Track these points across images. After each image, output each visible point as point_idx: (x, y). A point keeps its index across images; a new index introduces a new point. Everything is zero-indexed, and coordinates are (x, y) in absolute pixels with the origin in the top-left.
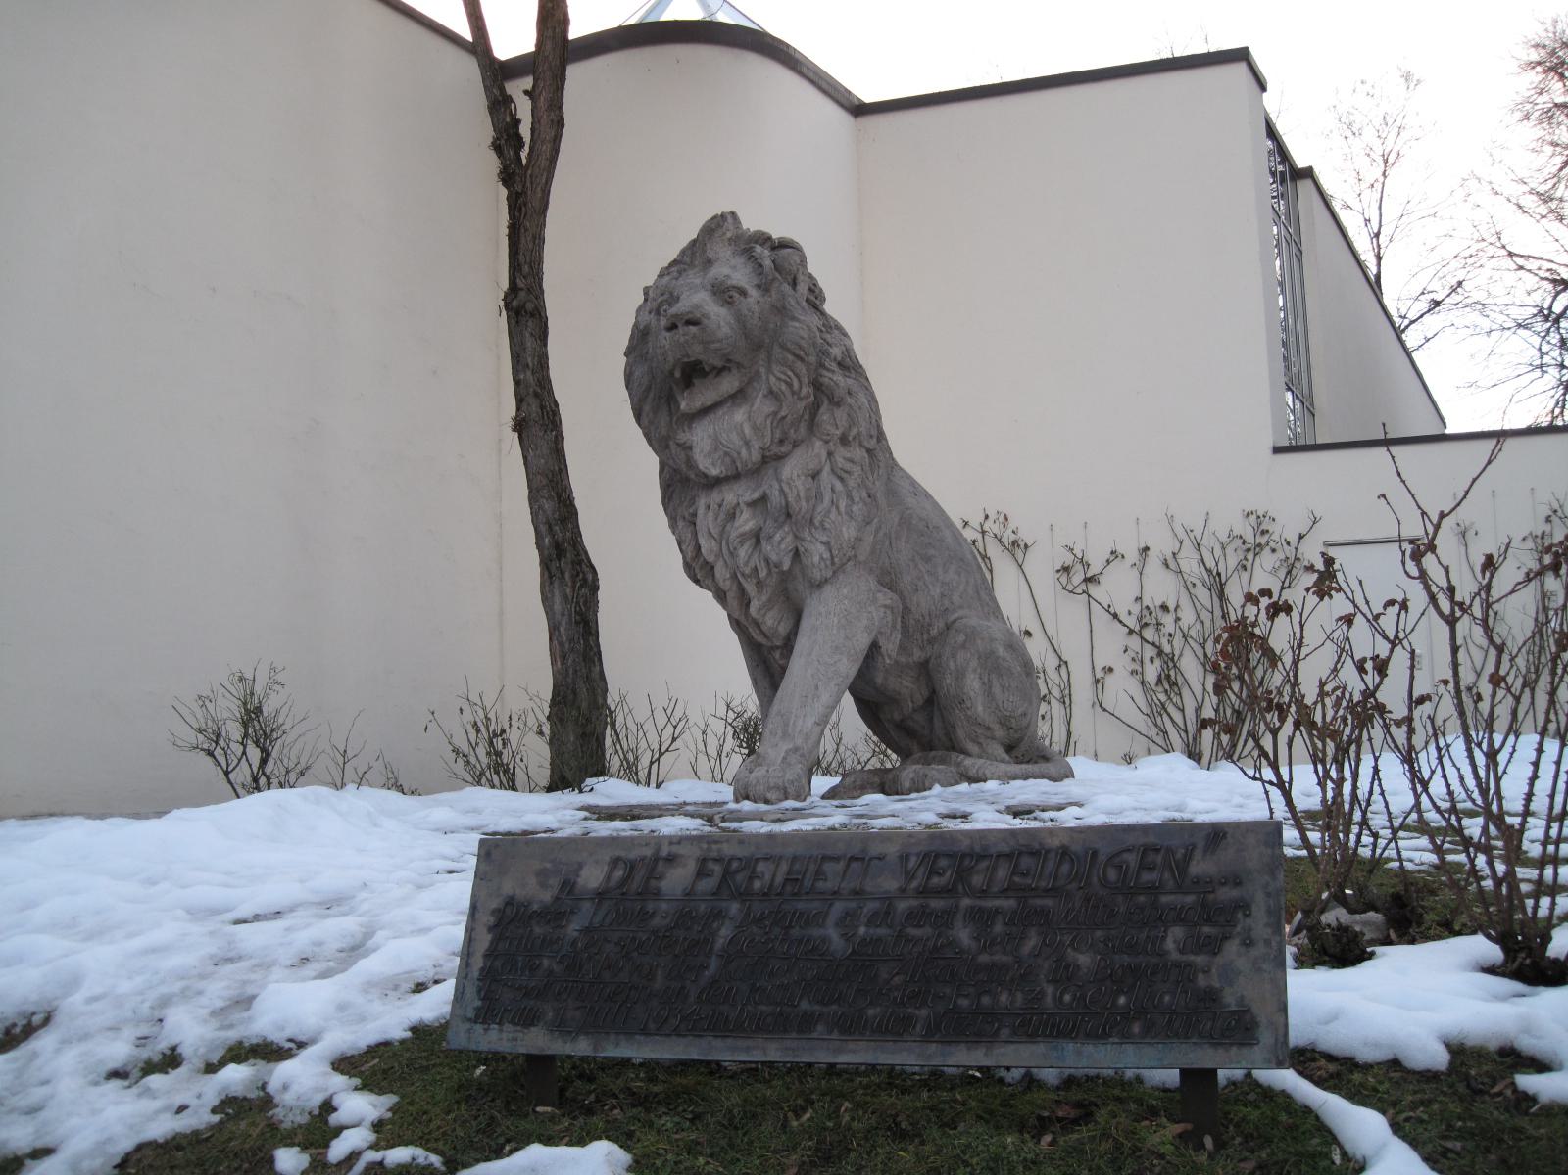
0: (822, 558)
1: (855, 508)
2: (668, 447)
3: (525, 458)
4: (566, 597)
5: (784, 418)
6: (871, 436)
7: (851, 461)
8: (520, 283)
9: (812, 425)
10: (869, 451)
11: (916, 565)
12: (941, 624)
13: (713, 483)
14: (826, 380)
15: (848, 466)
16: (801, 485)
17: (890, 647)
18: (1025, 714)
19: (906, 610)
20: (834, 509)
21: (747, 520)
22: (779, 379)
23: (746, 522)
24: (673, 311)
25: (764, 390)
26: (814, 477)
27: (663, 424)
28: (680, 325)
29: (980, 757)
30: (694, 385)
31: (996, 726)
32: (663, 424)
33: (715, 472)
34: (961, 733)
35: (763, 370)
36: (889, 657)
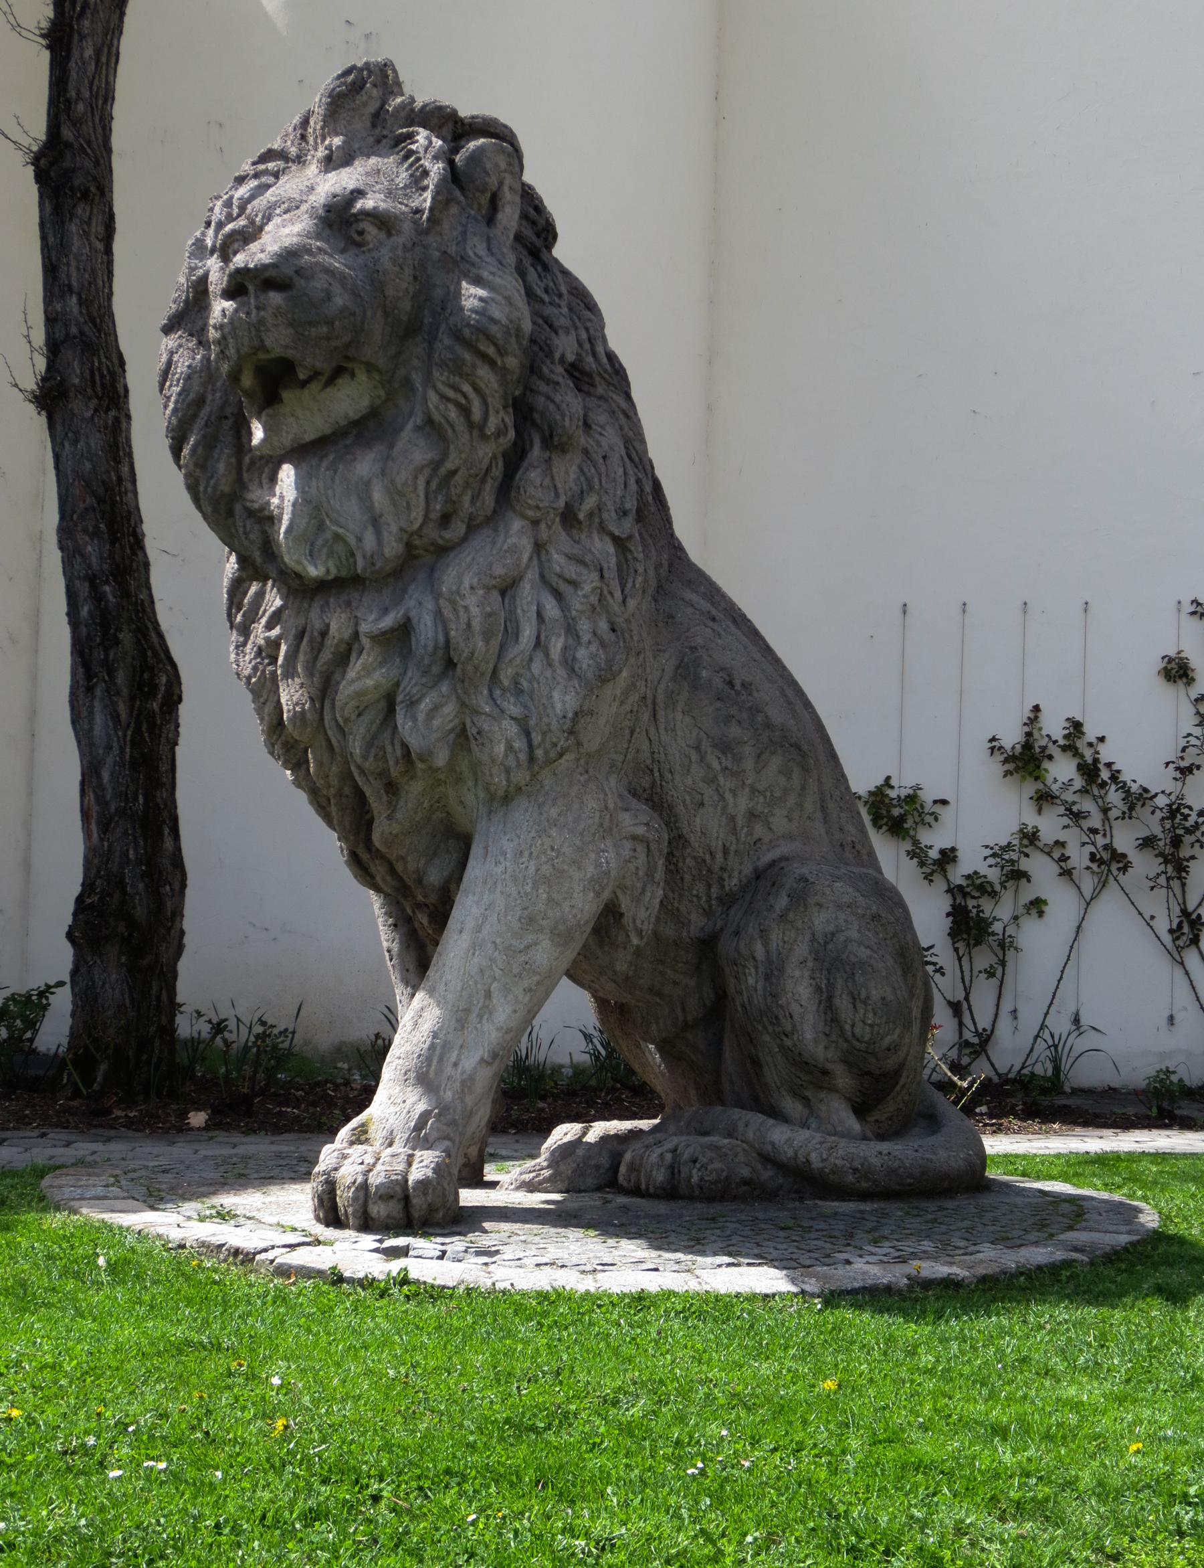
0: (510, 748)
1: (582, 653)
2: (230, 513)
3: (57, 457)
4: (115, 716)
5: (454, 473)
6: (625, 513)
7: (582, 562)
8: (67, 133)
9: (506, 491)
10: (616, 540)
11: (702, 759)
12: (748, 869)
14: (540, 402)
15: (571, 570)
16: (474, 605)
17: (642, 914)
18: (892, 1049)
19: (678, 841)
20: (539, 656)
21: (367, 671)
22: (444, 398)
24: (239, 260)
25: (418, 419)
26: (503, 593)
27: (221, 467)
28: (251, 288)
29: (804, 1125)
30: (281, 401)
32: (221, 467)
34: (771, 1076)
35: (417, 379)
36: (640, 933)
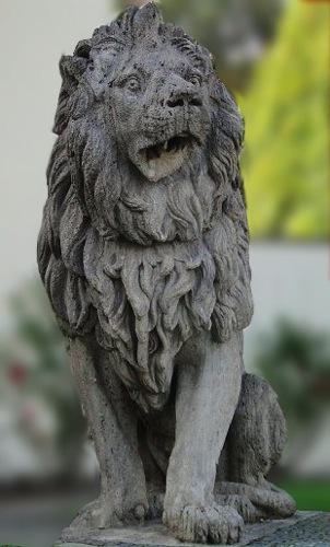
13: (154, 243)
23: (185, 284)
28: (186, 103)
31: (269, 462)
33: (163, 238)
